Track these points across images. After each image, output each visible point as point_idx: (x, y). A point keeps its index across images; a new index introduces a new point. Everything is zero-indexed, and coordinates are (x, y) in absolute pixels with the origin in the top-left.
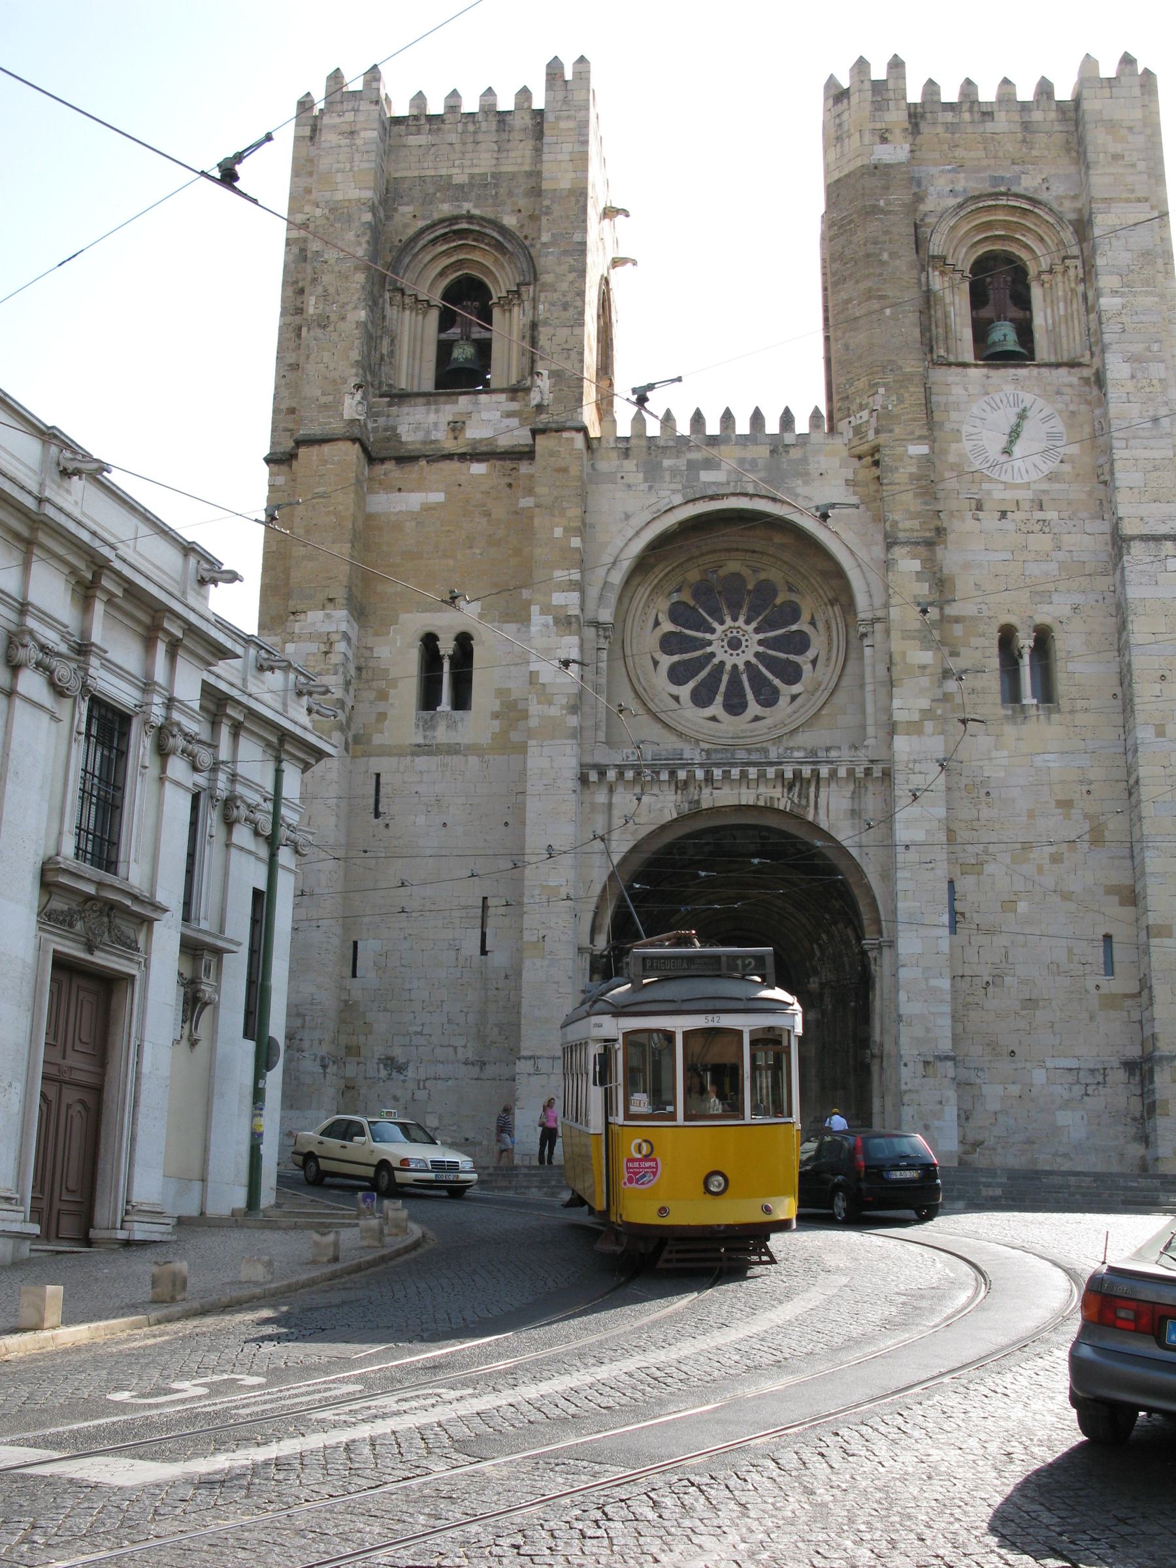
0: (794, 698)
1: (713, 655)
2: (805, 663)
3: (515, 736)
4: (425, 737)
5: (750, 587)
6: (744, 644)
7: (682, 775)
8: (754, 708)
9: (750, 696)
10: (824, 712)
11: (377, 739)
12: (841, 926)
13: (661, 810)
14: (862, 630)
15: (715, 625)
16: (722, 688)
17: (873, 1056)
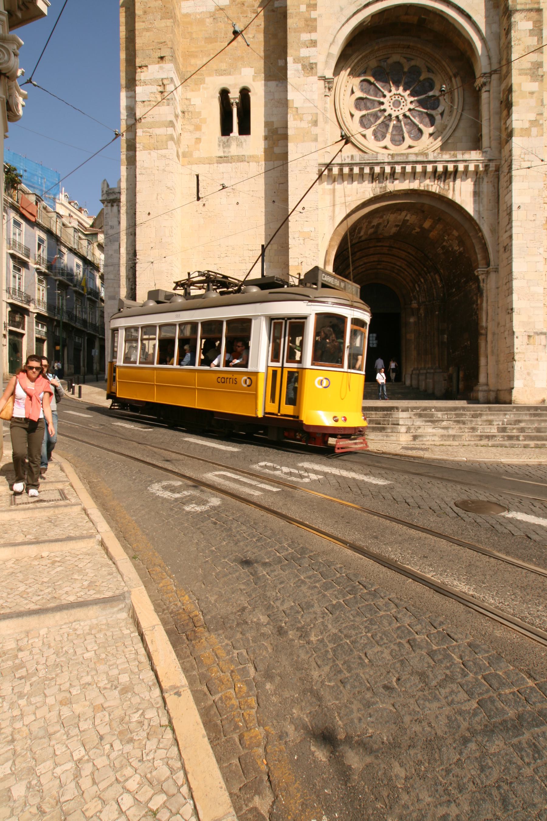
0: (431, 135)
1: (384, 110)
2: (437, 115)
3: (277, 150)
4: (224, 152)
5: (406, 70)
6: (402, 104)
7: (377, 170)
8: (408, 141)
9: (406, 135)
10: (449, 141)
11: (196, 154)
12: (432, 274)
13: (364, 192)
14: (483, 80)
15: (386, 93)
16: (390, 129)
17: (482, 334)
